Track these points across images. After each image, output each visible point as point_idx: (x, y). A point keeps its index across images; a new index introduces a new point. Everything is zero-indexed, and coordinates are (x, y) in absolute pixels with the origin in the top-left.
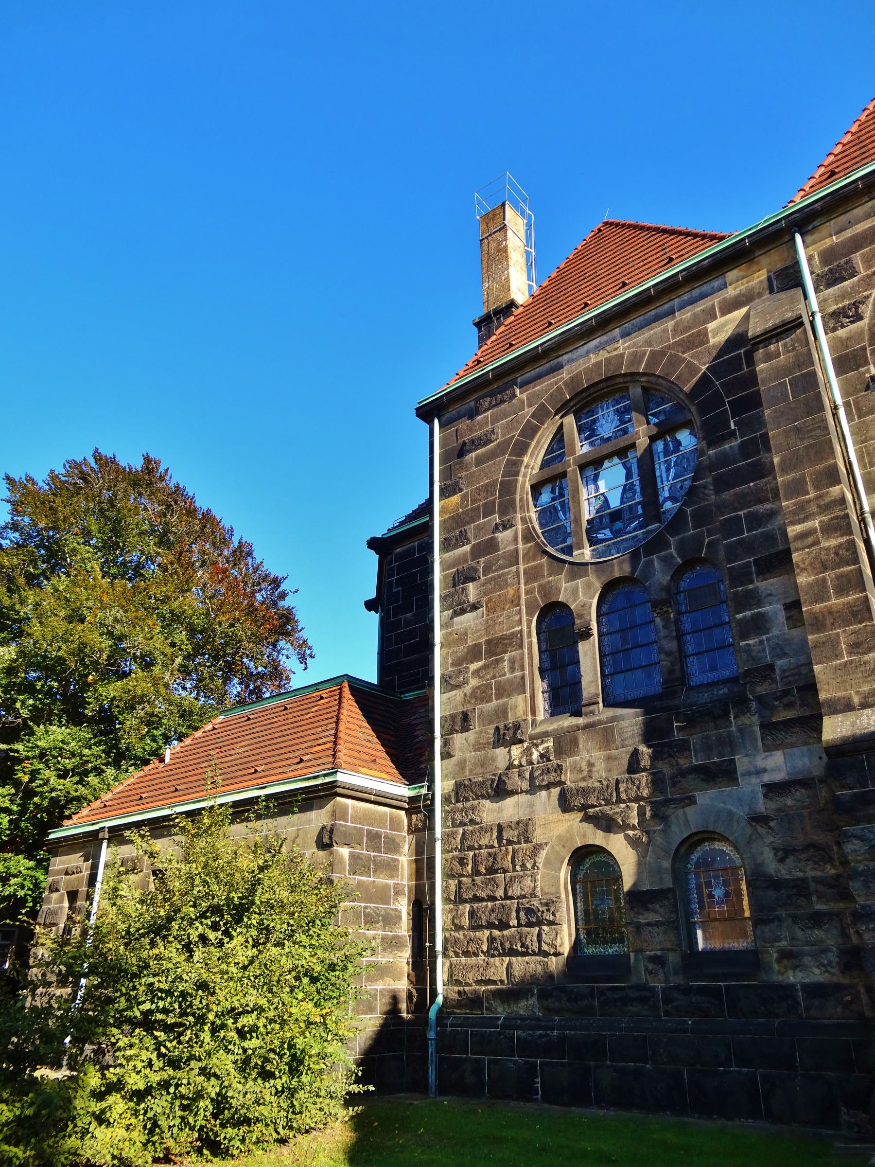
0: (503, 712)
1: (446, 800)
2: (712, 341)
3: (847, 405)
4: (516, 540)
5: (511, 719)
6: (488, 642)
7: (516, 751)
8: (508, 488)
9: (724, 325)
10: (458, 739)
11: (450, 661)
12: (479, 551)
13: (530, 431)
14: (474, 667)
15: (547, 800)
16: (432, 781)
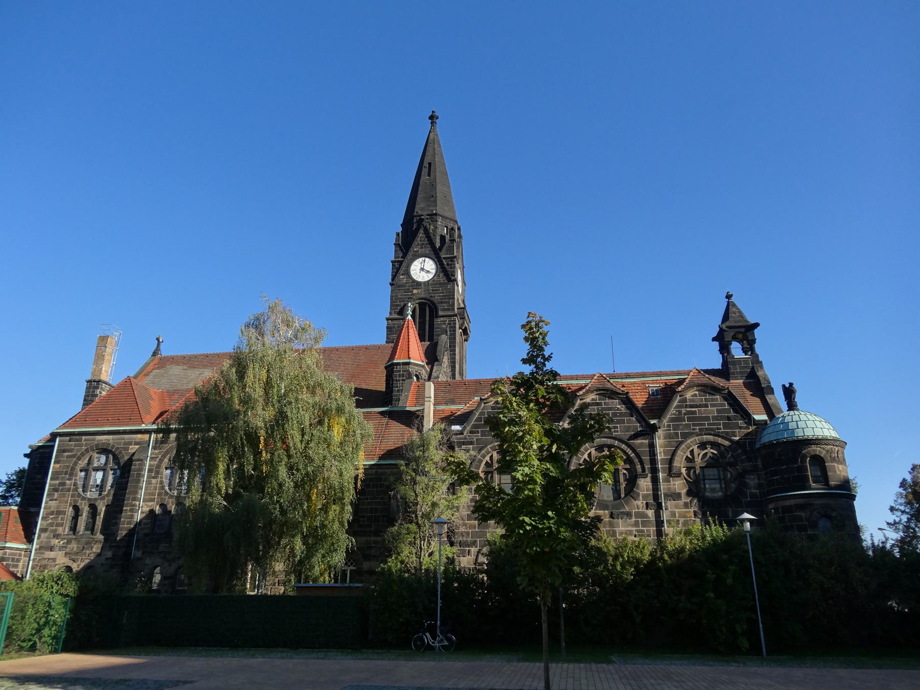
0: (56, 530)
1: (36, 550)
2: (129, 451)
3: (146, 481)
4: (71, 485)
5: (57, 533)
6: (57, 511)
7: (57, 541)
8: (73, 469)
9: (133, 448)
10: (43, 535)
11: (45, 513)
12: (60, 484)
13: (83, 454)
14: (51, 517)
15: (62, 553)
16: (33, 544)
